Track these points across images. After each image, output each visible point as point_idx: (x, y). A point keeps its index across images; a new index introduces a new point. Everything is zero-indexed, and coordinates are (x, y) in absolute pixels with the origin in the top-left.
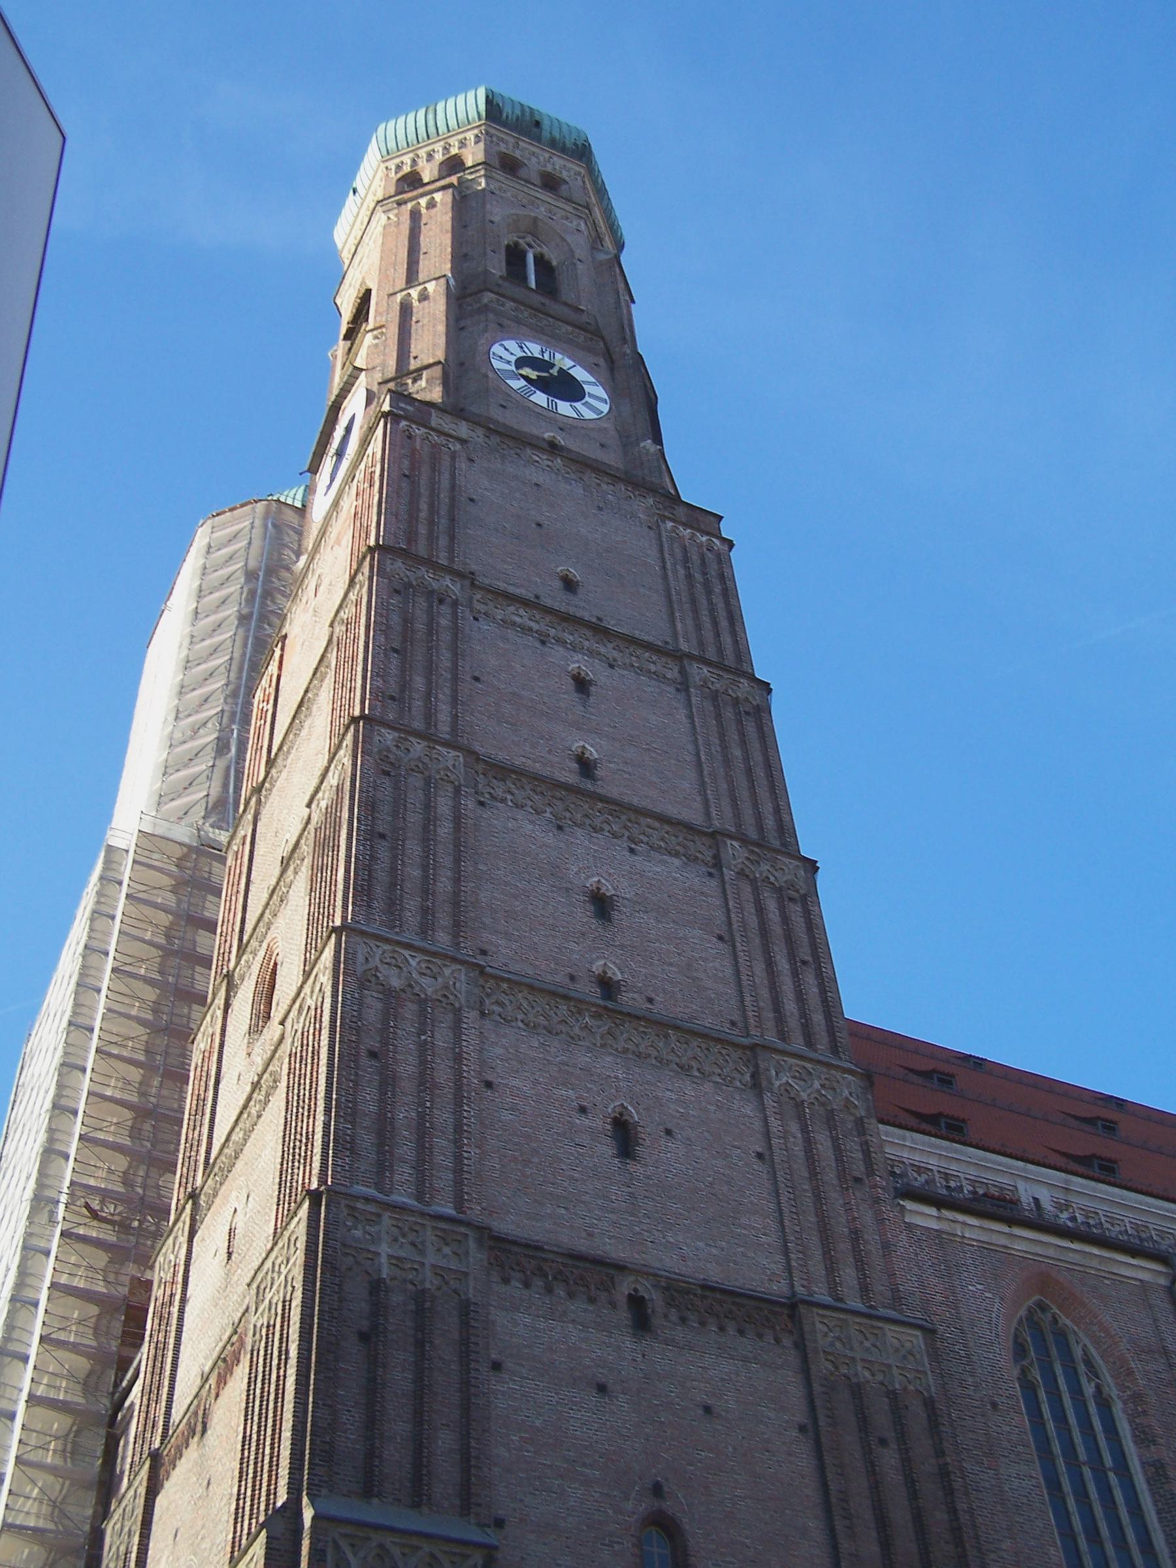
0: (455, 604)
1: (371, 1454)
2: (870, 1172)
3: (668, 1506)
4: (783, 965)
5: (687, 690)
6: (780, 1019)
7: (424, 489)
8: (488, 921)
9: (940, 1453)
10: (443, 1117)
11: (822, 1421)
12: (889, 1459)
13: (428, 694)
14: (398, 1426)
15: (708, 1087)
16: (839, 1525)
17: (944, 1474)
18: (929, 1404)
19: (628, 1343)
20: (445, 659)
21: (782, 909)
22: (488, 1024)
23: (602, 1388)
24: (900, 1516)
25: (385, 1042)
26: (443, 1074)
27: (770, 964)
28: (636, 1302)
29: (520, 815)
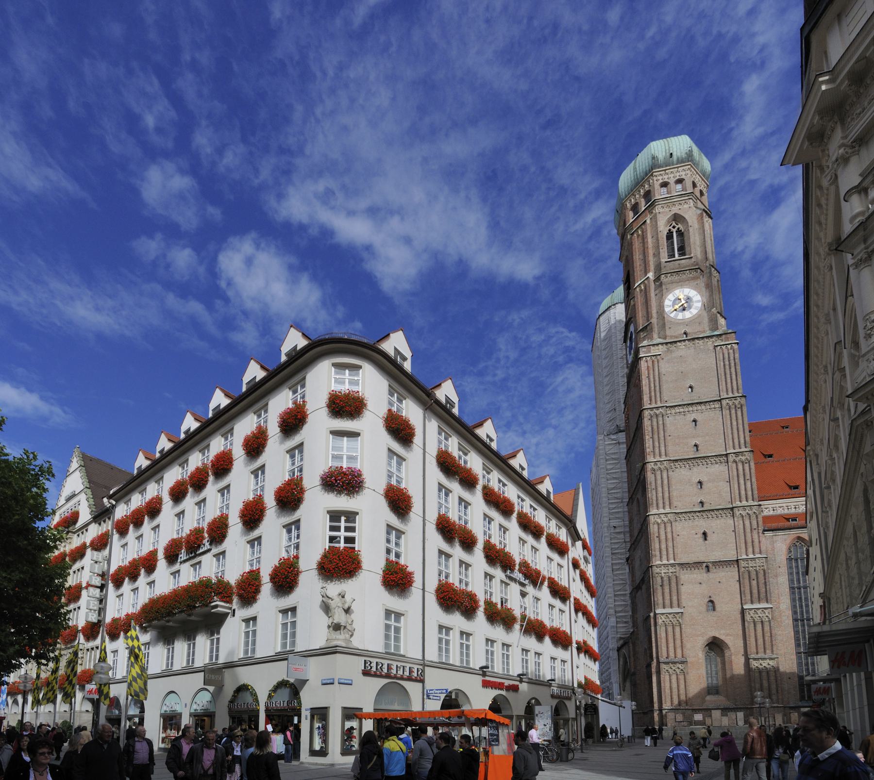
0: (663, 416)
1: (664, 603)
2: (758, 527)
3: (712, 599)
4: (742, 482)
5: (722, 410)
6: (740, 497)
7: (652, 380)
9: (765, 579)
10: (670, 544)
11: (741, 579)
12: (754, 583)
13: (659, 447)
14: (667, 597)
15: (722, 520)
16: (742, 595)
17: (765, 583)
18: (764, 571)
19: (705, 575)
22: (677, 523)
23: (700, 583)
24: (755, 591)
25: (659, 534)
26: (669, 536)
27: (739, 484)
28: (707, 567)
29: (681, 470)
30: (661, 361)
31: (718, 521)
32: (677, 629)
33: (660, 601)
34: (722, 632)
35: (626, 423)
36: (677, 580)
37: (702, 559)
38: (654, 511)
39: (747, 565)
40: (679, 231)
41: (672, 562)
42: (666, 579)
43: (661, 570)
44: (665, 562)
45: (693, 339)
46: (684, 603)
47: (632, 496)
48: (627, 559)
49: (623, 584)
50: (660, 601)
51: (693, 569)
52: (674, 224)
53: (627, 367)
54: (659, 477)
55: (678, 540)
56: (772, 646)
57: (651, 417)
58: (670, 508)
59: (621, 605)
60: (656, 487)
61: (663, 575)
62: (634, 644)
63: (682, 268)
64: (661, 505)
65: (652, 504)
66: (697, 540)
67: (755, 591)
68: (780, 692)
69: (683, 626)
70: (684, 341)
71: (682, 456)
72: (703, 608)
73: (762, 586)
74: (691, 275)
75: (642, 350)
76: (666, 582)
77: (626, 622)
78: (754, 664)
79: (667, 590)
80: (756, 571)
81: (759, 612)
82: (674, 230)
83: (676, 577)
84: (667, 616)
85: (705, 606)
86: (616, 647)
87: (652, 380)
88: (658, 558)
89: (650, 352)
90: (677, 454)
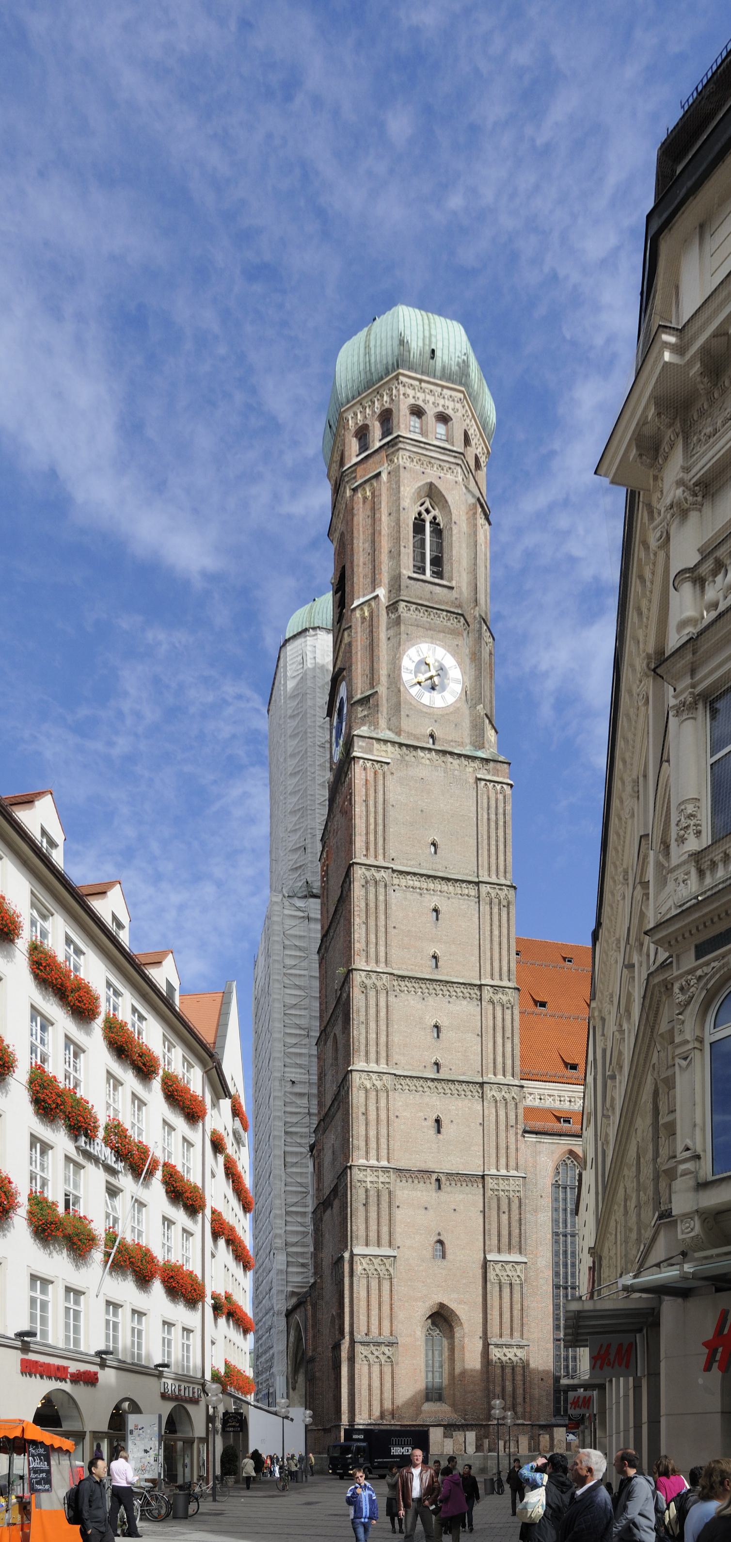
8: (397, 1050)
14: (373, 1227)
19: (434, 1194)
20: (382, 922)
21: (503, 1014)
23: (426, 1208)
25: (366, 1110)
28: (438, 1180)
30: (389, 777)
31: (460, 1103)
32: (386, 1285)
33: (362, 1232)
34: (454, 1296)
35: (323, 882)
36: (390, 1197)
37: (431, 1166)
38: (361, 1064)
39: (496, 1187)
40: (434, 522)
41: (384, 1163)
42: (372, 1193)
43: (366, 1176)
44: (373, 1162)
45: (445, 753)
46: (398, 1240)
47: (326, 1027)
48: (312, 1148)
49: (303, 1192)
50: (362, 1232)
51: (416, 1181)
52: (427, 504)
53: (331, 769)
54: (372, 1002)
55: (396, 1124)
56: (522, 1325)
57: (367, 882)
58: (387, 1064)
59: (297, 1232)
60: (367, 1019)
61: (369, 1185)
62: (314, 1306)
63: (436, 602)
64: (373, 1055)
65: (359, 1051)
66: (425, 1130)
67: (505, 1232)
68: (527, 1400)
69: (395, 1281)
70: (430, 750)
71: (412, 970)
72: (428, 1253)
73: (515, 1224)
74: (449, 624)
75: (358, 744)
76: (373, 1200)
77: (303, 1265)
78: (496, 1354)
79: (373, 1215)
80: (509, 1199)
81: (508, 1267)
82: (428, 518)
83: (390, 1192)
84: (370, 1260)
85: (430, 1248)
86: (284, 1309)
87: (372, 809)
88: (363, 1152)
89: (370, 751)
90: (404, 967)
